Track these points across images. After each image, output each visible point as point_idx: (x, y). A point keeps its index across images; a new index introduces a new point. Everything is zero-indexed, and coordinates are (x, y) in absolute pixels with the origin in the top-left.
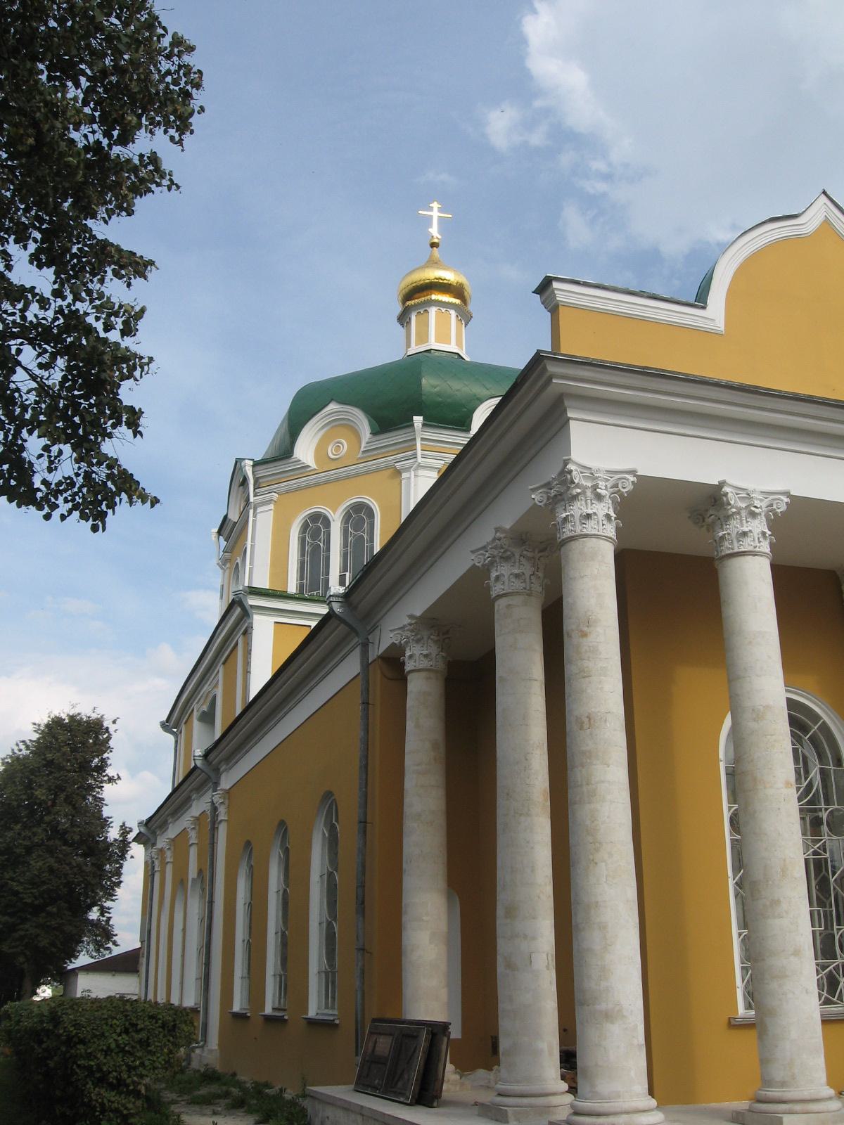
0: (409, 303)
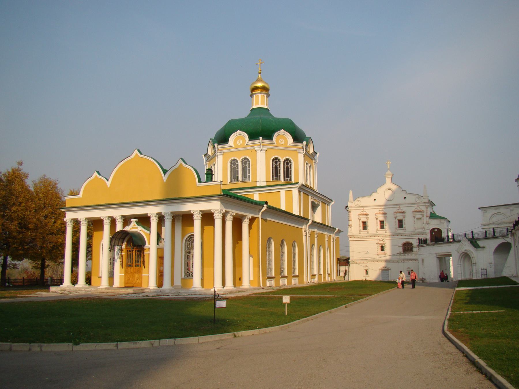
0: (254, 93)
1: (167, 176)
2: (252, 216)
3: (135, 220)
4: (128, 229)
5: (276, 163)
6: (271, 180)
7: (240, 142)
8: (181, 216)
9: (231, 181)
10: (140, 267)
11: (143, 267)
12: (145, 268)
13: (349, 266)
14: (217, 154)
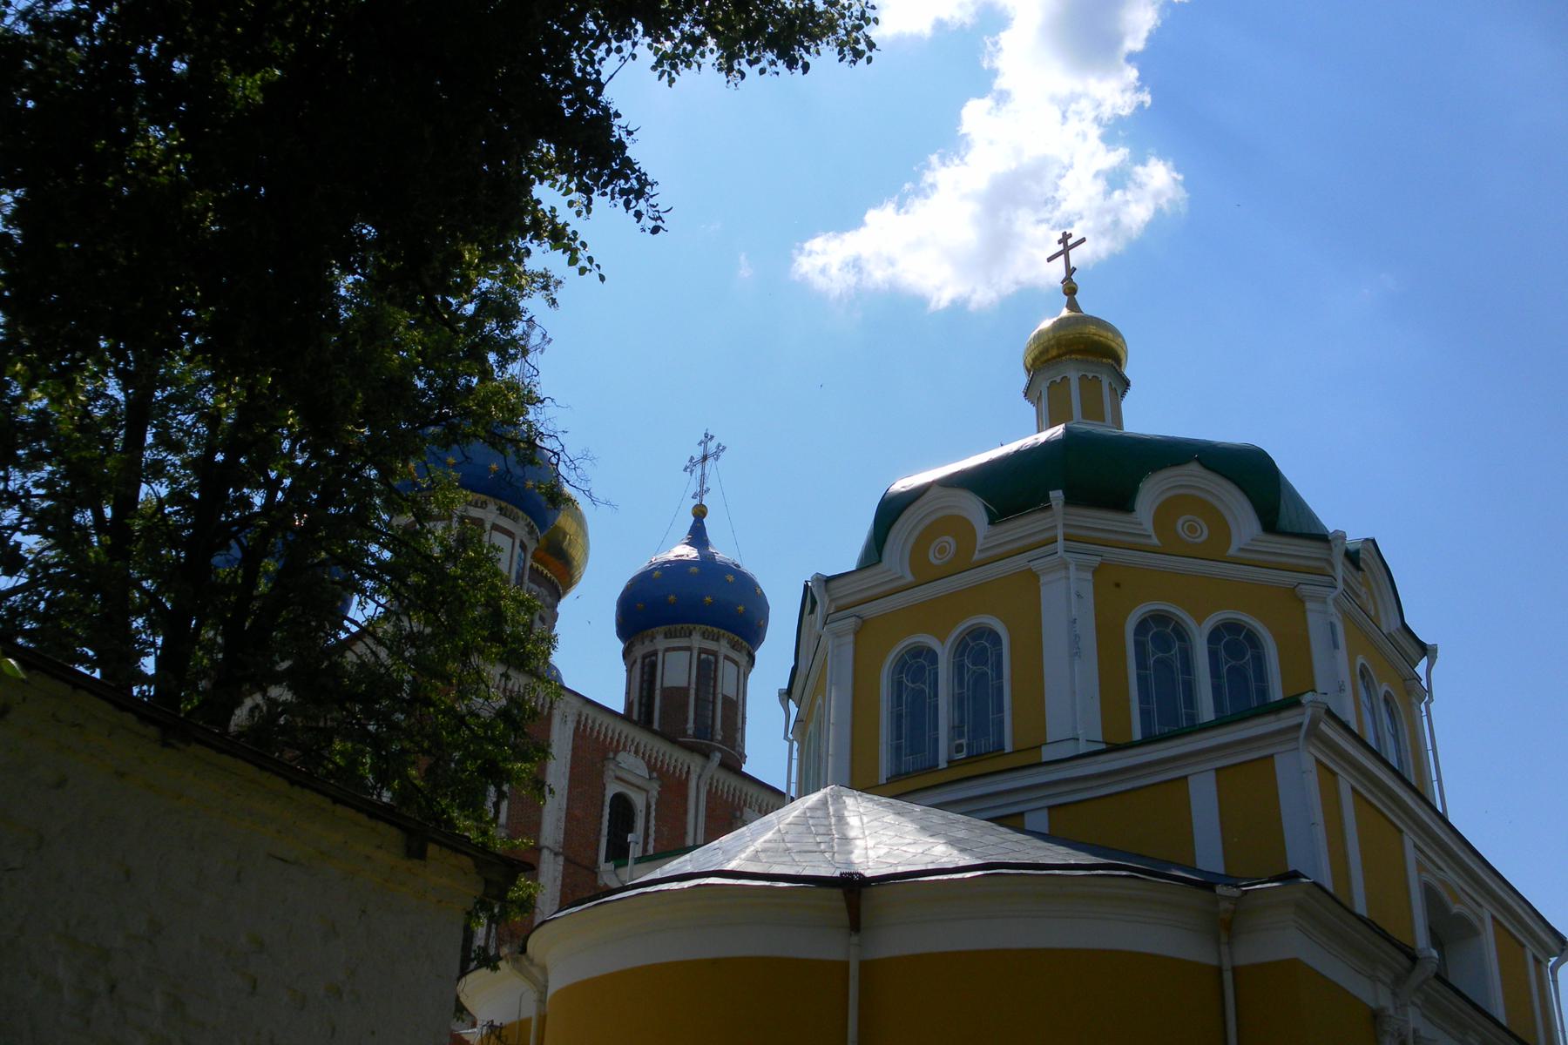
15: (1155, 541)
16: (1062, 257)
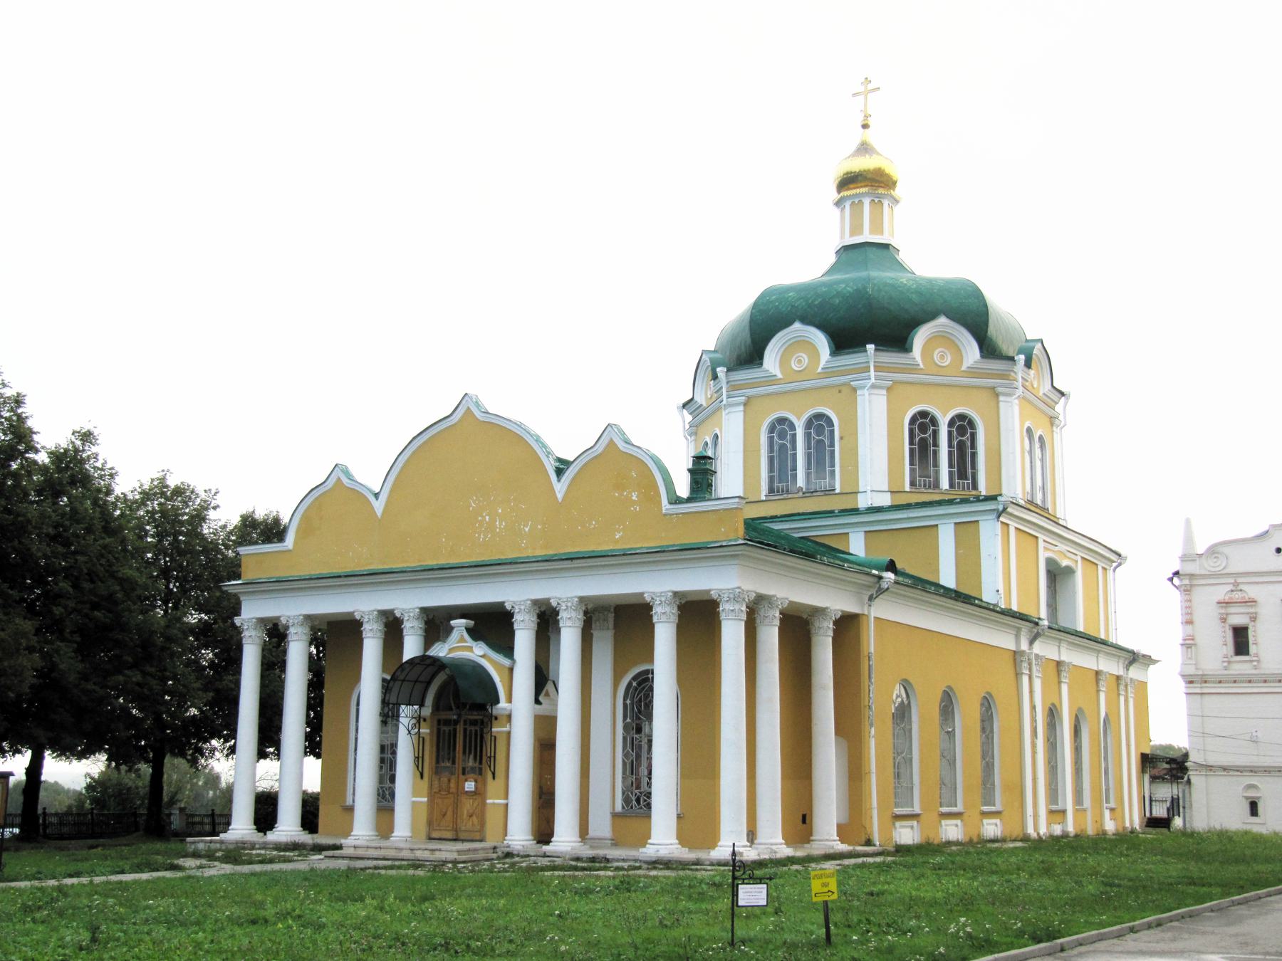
1: (567, 483)
2: (842, 611)
3: (463, 621)
4: (440, 651)
5: (923, 428)
6: (907, 488)
7: (800, 361)
8: (612, 610)
9: (771, 490)
10: (480, 773)
11: (490, 775)
12: (494, 778)
13: (1189, 782)
14: (724, 402)
15: (922, 366)
16: (861, 98)
